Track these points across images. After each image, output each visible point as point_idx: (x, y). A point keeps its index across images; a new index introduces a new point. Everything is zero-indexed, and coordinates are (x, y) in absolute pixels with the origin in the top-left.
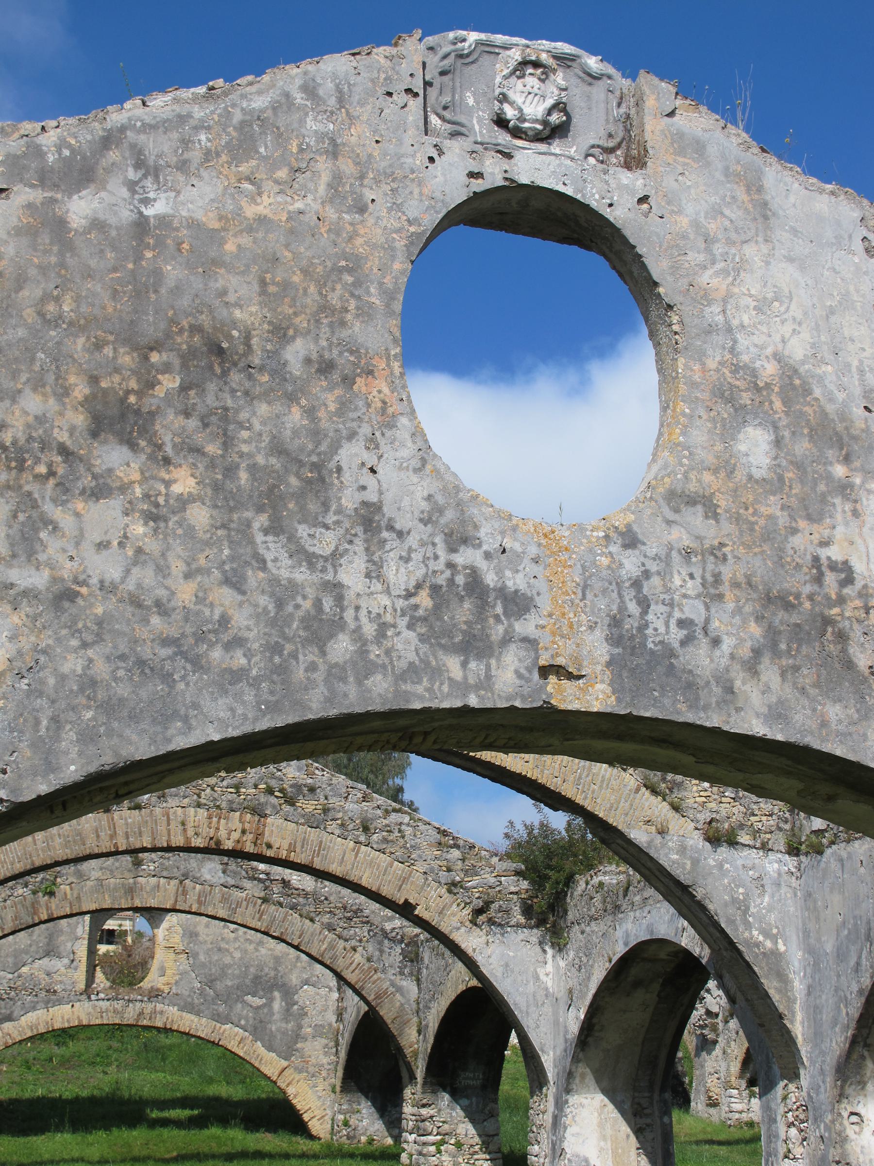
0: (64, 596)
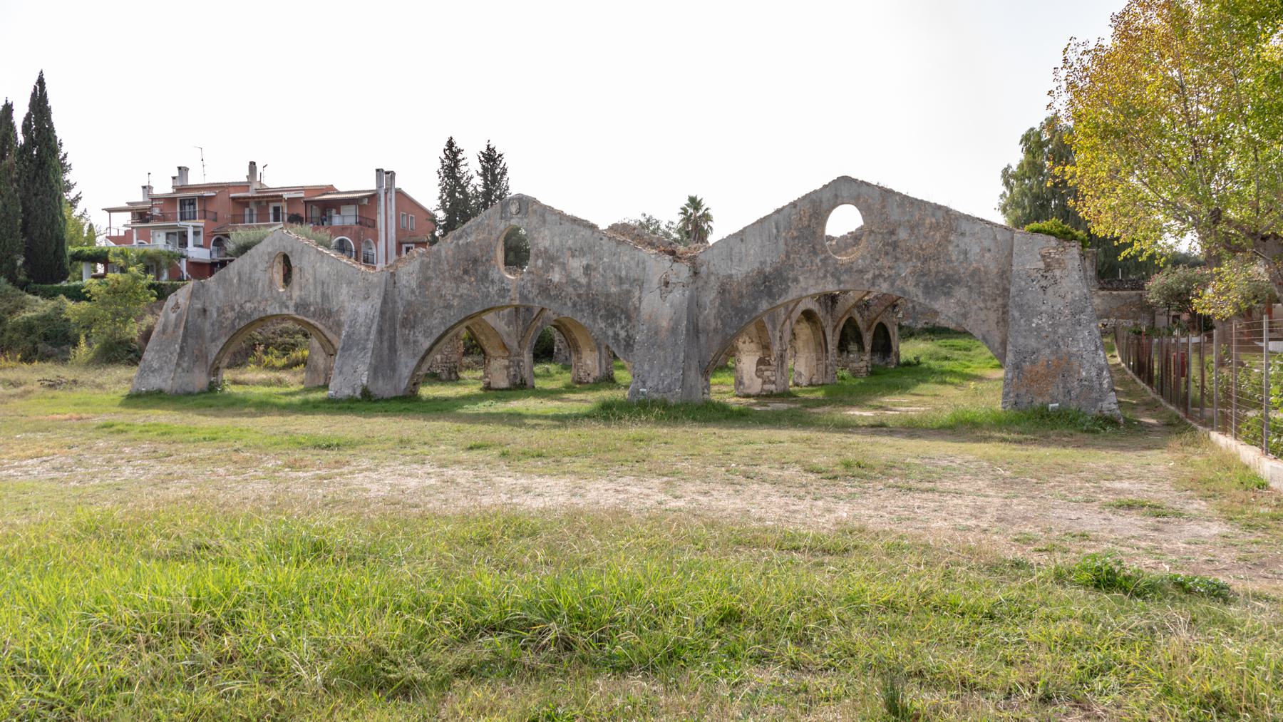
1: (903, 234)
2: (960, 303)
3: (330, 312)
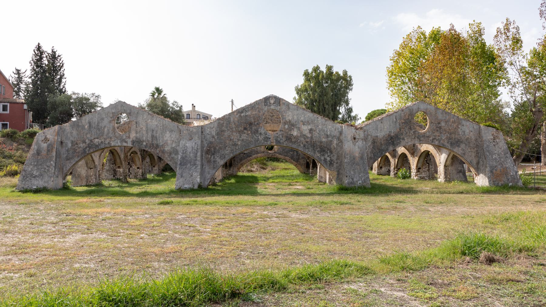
0: (243, 140)
1: (443, 124)
2: (463, 150)
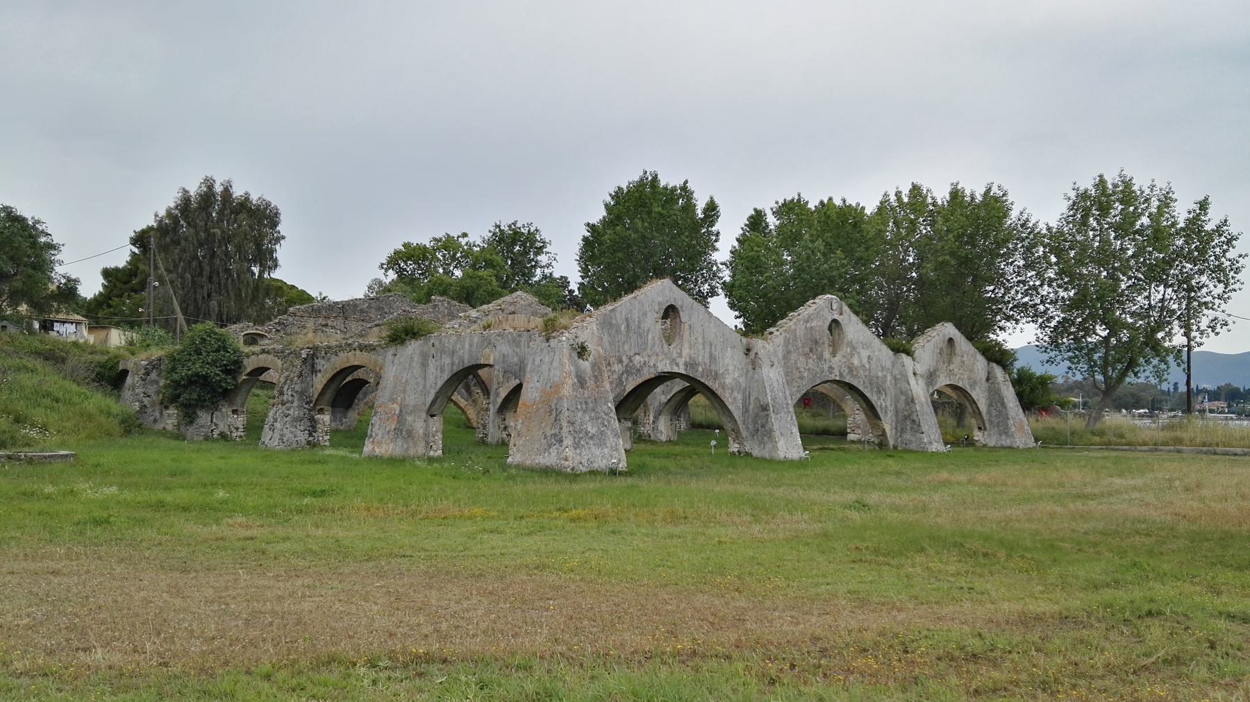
3: (716, 374)
